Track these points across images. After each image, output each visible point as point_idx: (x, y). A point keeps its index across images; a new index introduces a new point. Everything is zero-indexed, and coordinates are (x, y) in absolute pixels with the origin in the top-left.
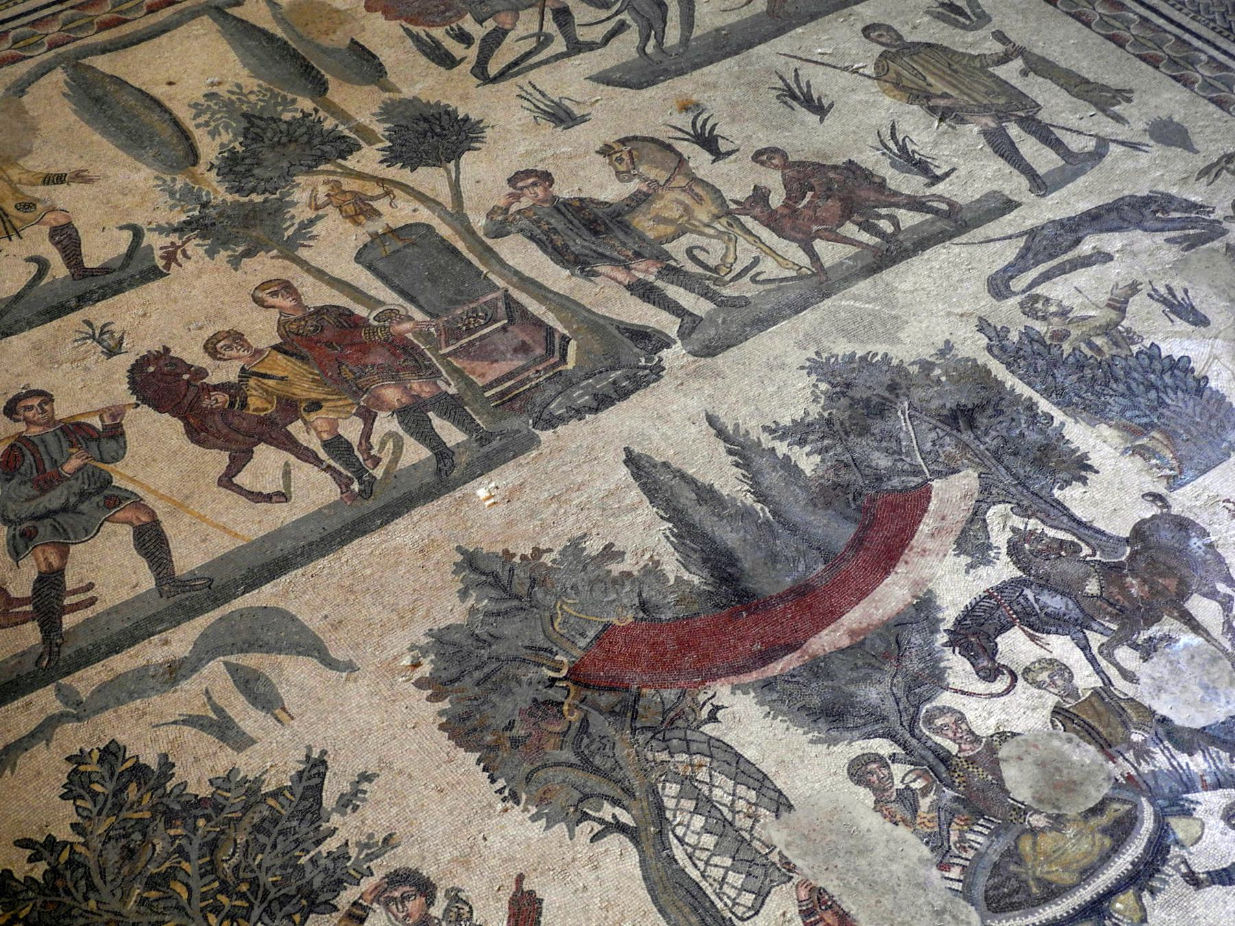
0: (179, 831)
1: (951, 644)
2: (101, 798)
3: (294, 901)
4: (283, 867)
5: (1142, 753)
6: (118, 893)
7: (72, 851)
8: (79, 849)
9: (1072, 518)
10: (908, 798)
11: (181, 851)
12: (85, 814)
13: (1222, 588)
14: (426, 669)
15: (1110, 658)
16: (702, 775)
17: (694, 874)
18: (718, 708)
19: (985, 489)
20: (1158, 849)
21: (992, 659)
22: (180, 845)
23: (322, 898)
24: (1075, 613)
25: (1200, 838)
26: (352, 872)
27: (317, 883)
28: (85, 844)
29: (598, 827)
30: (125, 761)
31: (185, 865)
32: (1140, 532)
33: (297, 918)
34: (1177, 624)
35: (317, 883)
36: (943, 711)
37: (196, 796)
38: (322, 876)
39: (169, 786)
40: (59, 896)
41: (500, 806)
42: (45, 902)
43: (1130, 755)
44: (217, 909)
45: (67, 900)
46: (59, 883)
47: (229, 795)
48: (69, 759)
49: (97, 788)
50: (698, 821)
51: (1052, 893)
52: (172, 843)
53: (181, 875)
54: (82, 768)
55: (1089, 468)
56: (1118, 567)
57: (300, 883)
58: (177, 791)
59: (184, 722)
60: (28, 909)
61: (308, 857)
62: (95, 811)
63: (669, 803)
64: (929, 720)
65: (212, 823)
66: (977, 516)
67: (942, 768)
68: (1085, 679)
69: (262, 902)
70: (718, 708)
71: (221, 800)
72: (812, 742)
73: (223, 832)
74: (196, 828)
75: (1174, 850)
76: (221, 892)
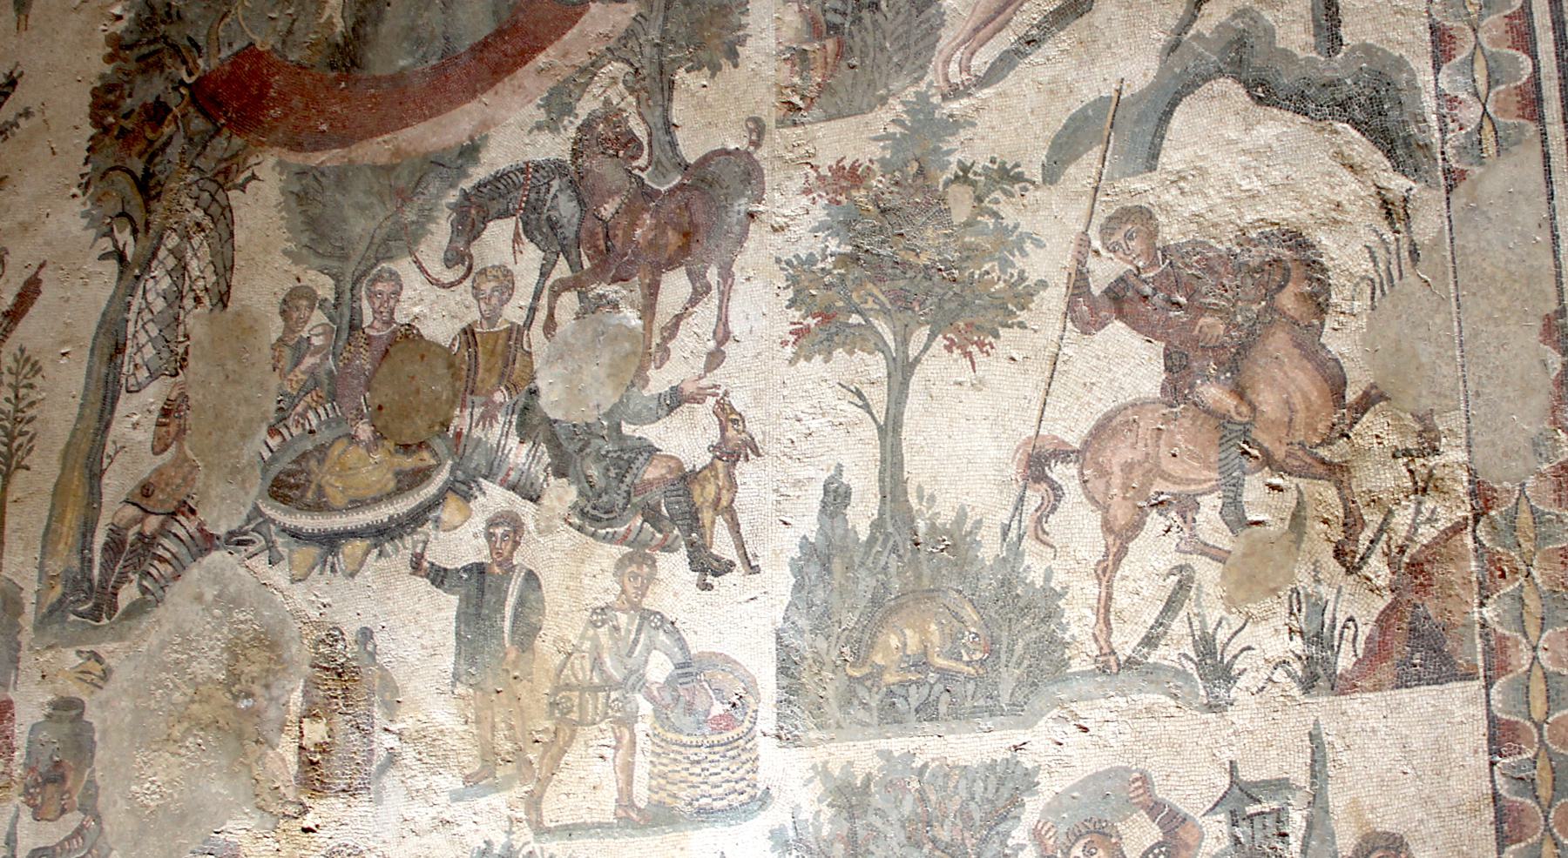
1: (451, 207)
5: (488, 418)
9: (666, 111)
10: (301, 349)
13: (713, 275)
14: (120, 27)
15: (555, 295)
16: (196, 241)
17: (131, 329)
18: (254, 177)
19: (630, 34)
20: (417, 518)
21: (468, 243)
24: (570, 232)
25: (456, 528)
29: (111, 248)
32: (705, 160)
34: (638, 295)
36: (394, 276)
41: (75, 190)
43: (478, 411)
50: (166, 283)
51: (321, 507)
55: (733, 55)
56: (651, 195)
63: (162, 253)
64: (374, 281)
66: (589, 71)
67: (344, 336)
68: (514, 313)
70: (254, 177)
72: (286, 253)
75: (430, 525)
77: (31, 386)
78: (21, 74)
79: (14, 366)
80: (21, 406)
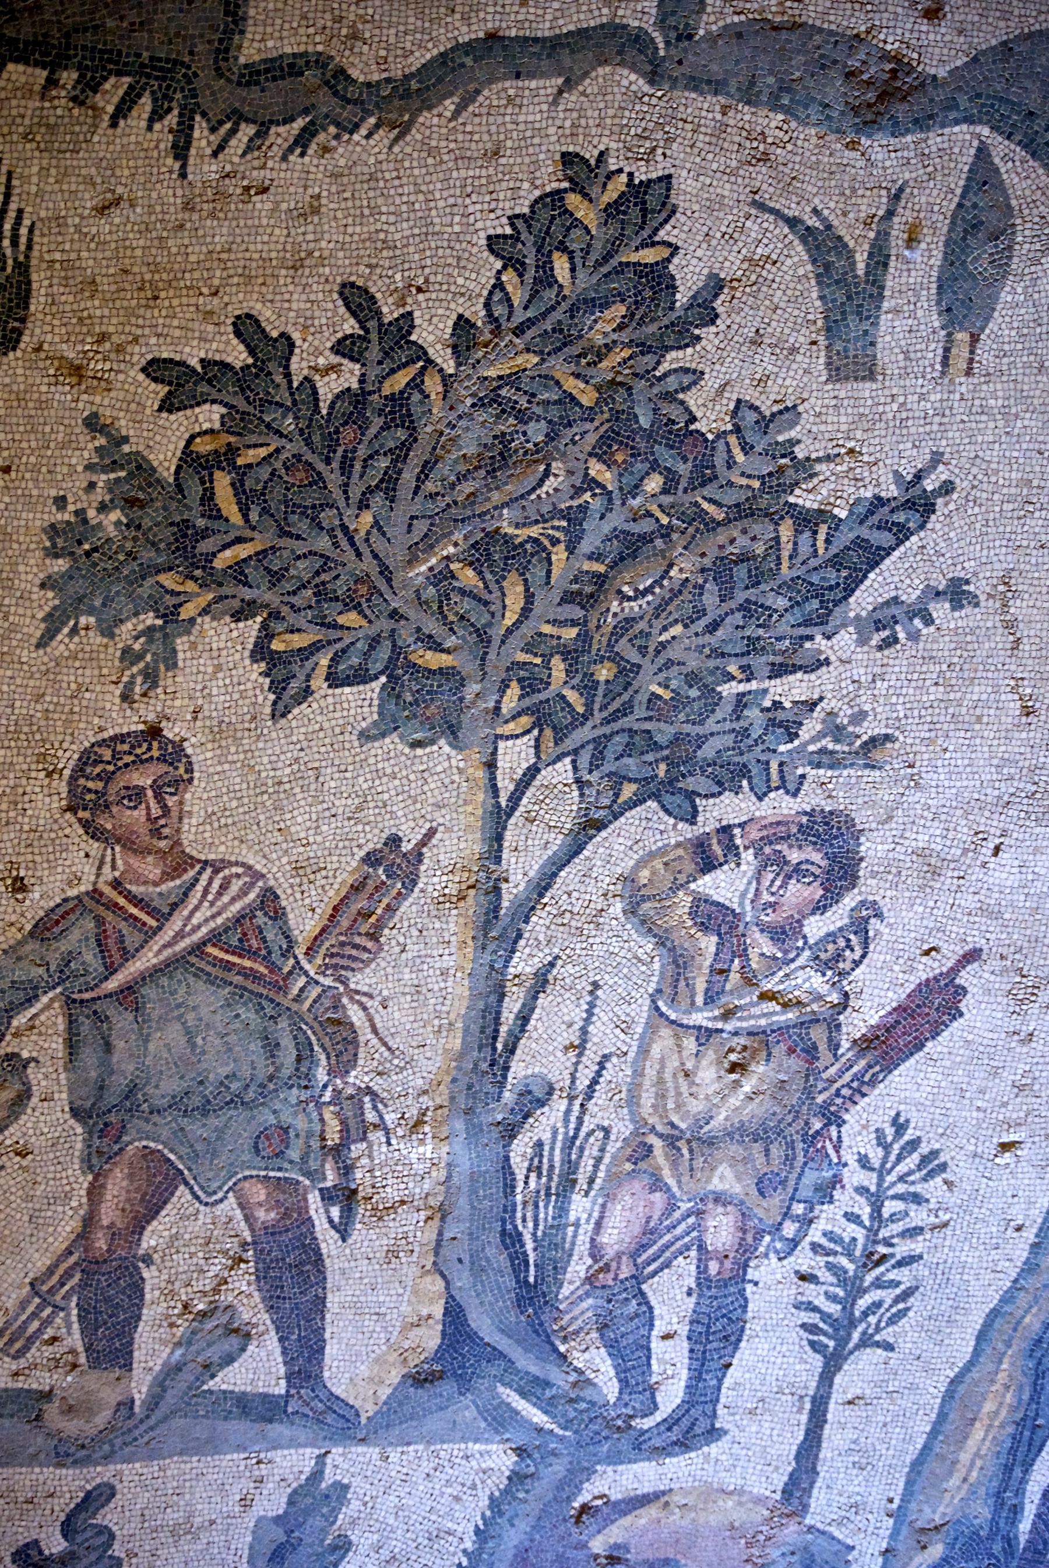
0: (607, 477)
2: (550, 294)
3: (650, 757)
4: (691, 679)
6: (421, 527)
7: (416, 384)
8: (433, 385)
11: (575, 518)
12: (499, 311)
22: (584, 508)
23: (690, 783)
26: (774, 766)
27: (708, 751)
28: (446, 380)
30: (650, 243)
31: (559, 554)
33: (628, 791)
35: (708, 751)
37: (693, 419)
38: (729, 740)
39: (673, 359)
40: (328, 461)
42: (298, 457)
44: (531, 684)
45: (333, 478)
46: (348, 434)
47: (740, 458)
48: (568, 159)
49: (561, 266)
52: (578, 491)
53: (537, 572)
54: (573, 200)
57: (687, 728)
58: (672, 383)
59: (807, 235)
60: (263, 452)
61: (742, 688)
62: (520, 316)
65: (666, 500)
69: (607, 721)
71: (720, 459)
73: (666, 533)
74: (635, 489)
76: (567, 653)
77: (917, 1199)
78: (947, 488)
79: (876, 1156)
80: (884, 1233)
